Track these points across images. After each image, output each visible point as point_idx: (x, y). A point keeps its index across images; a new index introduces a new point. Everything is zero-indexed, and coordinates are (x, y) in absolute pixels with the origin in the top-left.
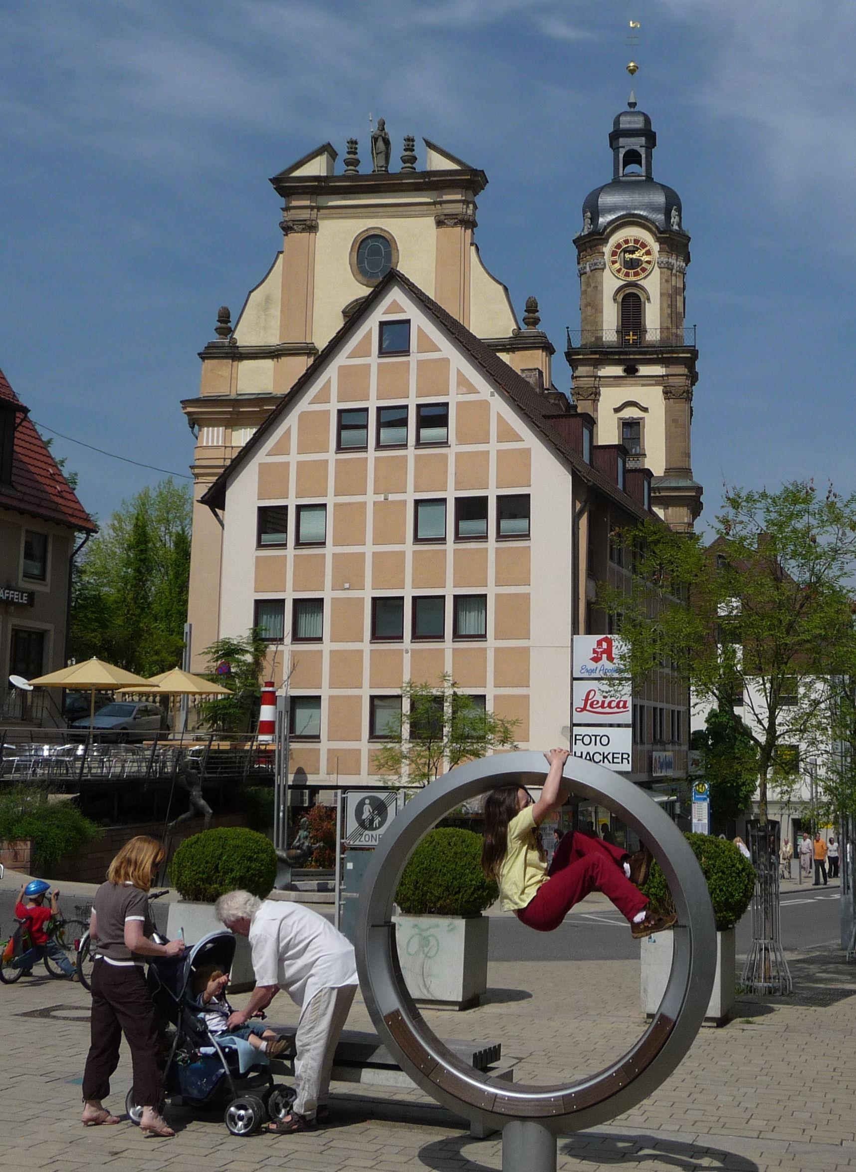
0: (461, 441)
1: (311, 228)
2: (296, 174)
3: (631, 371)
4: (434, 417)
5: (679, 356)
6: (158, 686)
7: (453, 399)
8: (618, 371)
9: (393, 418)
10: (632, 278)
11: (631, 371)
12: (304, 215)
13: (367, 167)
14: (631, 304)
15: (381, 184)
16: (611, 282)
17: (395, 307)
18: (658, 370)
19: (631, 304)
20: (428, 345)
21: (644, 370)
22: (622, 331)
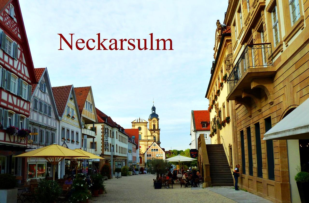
0: (159, 151)
1: (134, 126)
2: (133, 122)
3: (154, 132)
4: (157, 150)
5: (159, 130)
6: (89, 157)
7: (158, 149)
8: (153, 132)
9: (155, 150)
10: (154, 123)
11: (154, 132)
12: (134, 125)
13: (138, 121)
14: (154, 126)
15: (140, 123)
16: (153, 124)
17: (154, 143)
18: (157, 132)
19: (154, 126)
20: (157, 146)
21: (156, 132)
22: (154, 128)
